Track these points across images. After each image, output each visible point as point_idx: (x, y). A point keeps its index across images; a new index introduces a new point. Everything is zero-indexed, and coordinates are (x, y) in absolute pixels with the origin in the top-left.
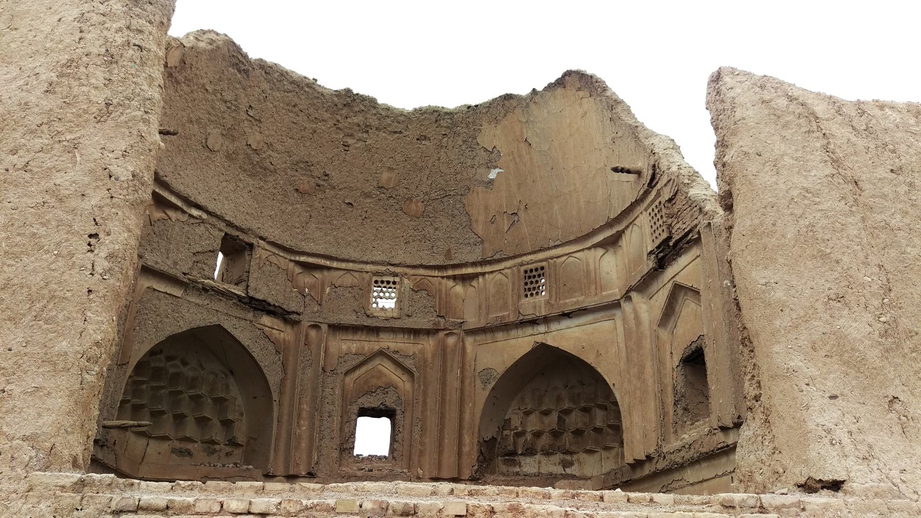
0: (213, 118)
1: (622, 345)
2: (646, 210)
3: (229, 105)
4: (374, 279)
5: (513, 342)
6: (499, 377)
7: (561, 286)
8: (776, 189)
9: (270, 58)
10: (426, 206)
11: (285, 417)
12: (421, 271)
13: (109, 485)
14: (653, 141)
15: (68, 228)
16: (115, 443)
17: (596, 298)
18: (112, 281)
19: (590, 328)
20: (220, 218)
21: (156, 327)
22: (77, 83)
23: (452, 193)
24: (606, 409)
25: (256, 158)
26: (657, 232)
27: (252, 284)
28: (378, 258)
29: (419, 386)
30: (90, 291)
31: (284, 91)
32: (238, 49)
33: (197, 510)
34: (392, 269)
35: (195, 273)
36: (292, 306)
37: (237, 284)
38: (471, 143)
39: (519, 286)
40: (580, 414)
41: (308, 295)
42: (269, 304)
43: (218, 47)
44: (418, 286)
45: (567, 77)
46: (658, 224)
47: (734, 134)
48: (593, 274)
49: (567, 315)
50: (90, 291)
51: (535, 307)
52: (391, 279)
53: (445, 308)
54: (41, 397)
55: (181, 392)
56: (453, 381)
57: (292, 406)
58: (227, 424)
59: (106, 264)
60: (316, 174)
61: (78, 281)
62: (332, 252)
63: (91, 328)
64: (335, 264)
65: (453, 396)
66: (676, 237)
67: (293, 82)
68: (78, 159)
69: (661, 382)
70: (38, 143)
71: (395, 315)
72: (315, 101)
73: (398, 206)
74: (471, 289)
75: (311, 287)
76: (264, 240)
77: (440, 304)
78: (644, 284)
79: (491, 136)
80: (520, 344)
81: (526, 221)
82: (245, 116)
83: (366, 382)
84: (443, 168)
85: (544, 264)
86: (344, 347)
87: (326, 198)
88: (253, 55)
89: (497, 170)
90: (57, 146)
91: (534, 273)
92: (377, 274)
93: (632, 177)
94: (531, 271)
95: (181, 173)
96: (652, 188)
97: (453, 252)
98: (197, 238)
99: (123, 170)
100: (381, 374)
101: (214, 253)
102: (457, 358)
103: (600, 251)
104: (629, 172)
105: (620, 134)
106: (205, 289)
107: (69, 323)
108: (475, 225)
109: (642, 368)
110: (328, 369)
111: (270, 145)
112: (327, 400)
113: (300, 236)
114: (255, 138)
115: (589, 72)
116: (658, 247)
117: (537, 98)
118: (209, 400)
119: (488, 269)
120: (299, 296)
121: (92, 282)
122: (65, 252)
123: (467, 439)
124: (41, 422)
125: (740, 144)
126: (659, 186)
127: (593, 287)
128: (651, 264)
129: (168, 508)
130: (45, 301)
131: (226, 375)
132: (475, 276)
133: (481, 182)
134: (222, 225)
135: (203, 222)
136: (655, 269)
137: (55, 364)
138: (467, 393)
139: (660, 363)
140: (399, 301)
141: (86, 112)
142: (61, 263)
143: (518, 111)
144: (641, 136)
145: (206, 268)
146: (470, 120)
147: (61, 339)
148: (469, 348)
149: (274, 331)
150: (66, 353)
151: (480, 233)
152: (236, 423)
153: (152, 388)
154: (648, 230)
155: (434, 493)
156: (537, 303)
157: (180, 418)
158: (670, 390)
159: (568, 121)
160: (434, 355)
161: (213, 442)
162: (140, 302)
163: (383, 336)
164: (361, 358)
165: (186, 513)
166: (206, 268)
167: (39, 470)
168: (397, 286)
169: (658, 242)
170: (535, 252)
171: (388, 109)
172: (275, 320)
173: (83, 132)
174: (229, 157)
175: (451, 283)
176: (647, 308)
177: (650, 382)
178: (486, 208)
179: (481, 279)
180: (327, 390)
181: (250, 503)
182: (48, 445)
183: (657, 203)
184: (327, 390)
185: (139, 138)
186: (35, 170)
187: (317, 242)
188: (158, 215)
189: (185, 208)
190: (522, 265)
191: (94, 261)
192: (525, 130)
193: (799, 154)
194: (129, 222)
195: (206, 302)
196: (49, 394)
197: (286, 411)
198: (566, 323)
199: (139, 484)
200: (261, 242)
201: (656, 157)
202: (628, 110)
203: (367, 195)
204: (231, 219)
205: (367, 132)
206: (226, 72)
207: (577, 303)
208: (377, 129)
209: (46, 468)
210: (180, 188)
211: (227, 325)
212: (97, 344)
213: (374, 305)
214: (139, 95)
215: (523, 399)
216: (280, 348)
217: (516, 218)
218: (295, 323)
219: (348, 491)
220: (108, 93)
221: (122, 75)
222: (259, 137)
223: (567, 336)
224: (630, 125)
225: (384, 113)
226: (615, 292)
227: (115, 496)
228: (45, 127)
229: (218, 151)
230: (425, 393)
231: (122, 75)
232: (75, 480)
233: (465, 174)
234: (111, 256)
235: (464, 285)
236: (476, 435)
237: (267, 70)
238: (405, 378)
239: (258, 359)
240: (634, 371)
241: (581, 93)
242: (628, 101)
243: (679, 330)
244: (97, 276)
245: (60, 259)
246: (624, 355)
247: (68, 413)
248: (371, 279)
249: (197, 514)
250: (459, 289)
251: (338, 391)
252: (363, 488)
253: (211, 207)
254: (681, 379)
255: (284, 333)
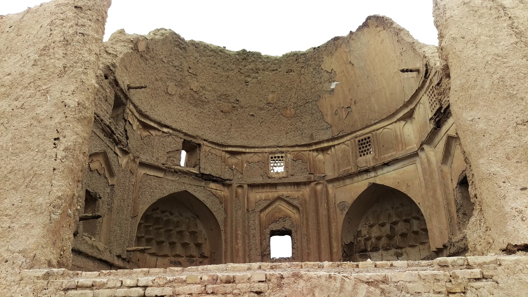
0: (169, 77)
1: (422, 178)
2: (425, 93)
3: (178, 68)
4: (271, 156)
5: (356, 184)
6: (350, 206)
7: (381, 146)
8: (476, 58)
9: (197, 39)
10: (296, 110)
11: (229, 239)
12: (297, 149)
13: (62, 274)
14: (424, 50)
15: (43, 136)
16: (139, 260)
17: (403, 152)
18: (67, 163)
19: (401, 170)
20: (179, 131)
21: (151, 195)
22: (48, 58)
23: (310, 101)
24: (419, 219)
25: (197, 96)
26: (433, 106)
27: (202, 166)
28: (271, 144)
29: (303, 215)
30: (54, 169)
31: (208, 56)
32: (178, 37)
33: (108, 286)
34: (280, 149)
35: (169, 163)
36: (227, 176)
37: (194, 167)
38: (318, 69)
39: (356, 150)
40: (403, 223)
41: (235, 169)
42: (213, 176)
43: (167, 37)
44: (296, 157)
45: (369, 21)
46: (433, 100)
47: (446, 28)
48: (399, 137)
49: (387, 164)
50: (54, 169)
51: (366, 162)
52: (280, 155)
53: (313, 168)
54: (29, 229)
55: (171, 230)
56: (323, 211)
57: (232, 232)
58: (198, 246)
59: (64, 154)
60: (232, 100)
61: (48, 164)
62: (245, 143)
63: (54, 189)
64: (248, 150)
65: (323, 219)
66: (444, 107)
67: (212, 50)
68: (49, 98)
69: (447, 199)
70: (28, 93)
71: (284, 175)
72: (226, 59)
73: (279, 113)
74: (328, 156)
75: (236, 165)
76: (206, 141)
77: (310, 167)
78: (430, 139)
79: (329, 63)
80: (361, 185)
81: (356, 111)
82: (187, 73)
83: (273, 216)
84: (304, 86)
85: (370, 135)
86: (258, 197)
87: (239, 114)
88: (187, 39)
89: (335, 83)
90: (38, 93)
91: (364, 141)
92: (271, 153)
93: (414, 74)
94: (362, 140)
95: (155, 109)
96: (427, 78)
97: (314, 135)
98: (168, 144)
99: (72, 102)
100: (280, 210)
101: (178, 151)
102: (324, 197)
103: (403, 123)
104: (411, 71)
105: (404, 49)
106: (176, 172)
107: (43, 188)
108: (325, 117)
109: (435, 191)
110: (250, 210)
111: (203, 88)
112: (251, 228)
113: (226, 137)
114: (195, 85)
115: (381, 15)
116: (435, 115)
117: (353, 36)
118: (187, 233)
119: (336, 142)
120: (230, 170)
121: (55, 164)
122: (42, 149)
123: (335, 244)
124: (28, 242)
125: (450, 33)
126: (430, 77)
127: (400, 145)
128: (432, 126)
129: (93, 286)
130: (31, 177)
131: (195, 218)
132: (329, 148)
133: (327, 92)
134: (181, 135)
135: (171, 134)
136: (435, 129)
137: (36, 210)
138: (332, 217)
139: (445, 186)
140: (286, 167)
141: (53, 73)
142: (40, 155)
143: (343, 46)
144: (416, 48)
145: (175, 160)
146: (316, 56)
147: (39, 196)
148: (330, 191)
149: (218, 191)
150: (41, 204)
151: (329, 122)
152: (203, 245)
153: (156, 229)
154: (428, 105)
155: (249, 269)
156: (367, 160)
157: (172, 244)
158: (453, 203)
159: (373, 47)
160: (310, 197)
161: (192, 256)
162: (140, 182)
163: (279, 188)
164: (268, 202)
165: (102, 288)
166: (175, 160)
167: (27, 269)
168: (284, 159)
169: (434, 111)
170: (363, 129)
171: (268, 57)
172: (218, 185)
173: (52, 84)
174: (181, 97)
175: (315, 154)
176: (433, 154)
177: (441, 199)
178: (331, 106)
179: (333, 149)
180: (251, 222)
181: (138, 280)
182: (32, 255)
183: (431, 87)
184: (251, 222)
185: (81, 83)
186: (27, 107)
187: (236, 139)
188: (145, 133)
189: (159, 128)
190: (356, 137)
191: (57, 153)
192: (349, 57)
193: (491, 33)
194: (77, 129)
195: (177, 179)
196: (33, 227)
197: (229, 236)
198: (386, 169)
199: (81, 274)
200: (205, 142)
201: (427, 59)
202: (408, 34)
203: (261, 109)
204: (186, 132)
205: (258, 73)
206: (173, 50)
207: (392, 156)
208: (263, 70)
209: (31, 267)
210: (156, 117)
211: (190, 191)
212: (59, 198)
213: (272, 171)
214: (81, 60)
215: (367, 218)
216: (222, 201)
217: (350, 110)
218: (229, 186)
219: (197, 270)
220: (65, 61)
221: (73, 50)
222: (196, 84)
223: (388, 177)
224: (410, 42)
225: (266, 61)
226: (414, 146)
227: (64, 281)
228: (32, 84)
229: (175, 94)
230: (307, 219)
231: (73, 50)
232: (44, 273)
233: (316, 88)
234: (66, 149)
235: (323, 154)
236: (340, 241)
237: (195, 45)
238: (294, 211)
239: (210, 208)
240: (430, 193)
241: (378, 29)
242: (407, 28)
243: (455, 165)
244: (58, 161)
245: (39, 153)
246: (423, 184)
247: (43, 237)
248: (269, 156)
249: (108, 288)
250: (320, 156)
251: (257, 222)
252: (206, 268)
253: (174, 126)
254: (459, 195)
255: (224, 192)
